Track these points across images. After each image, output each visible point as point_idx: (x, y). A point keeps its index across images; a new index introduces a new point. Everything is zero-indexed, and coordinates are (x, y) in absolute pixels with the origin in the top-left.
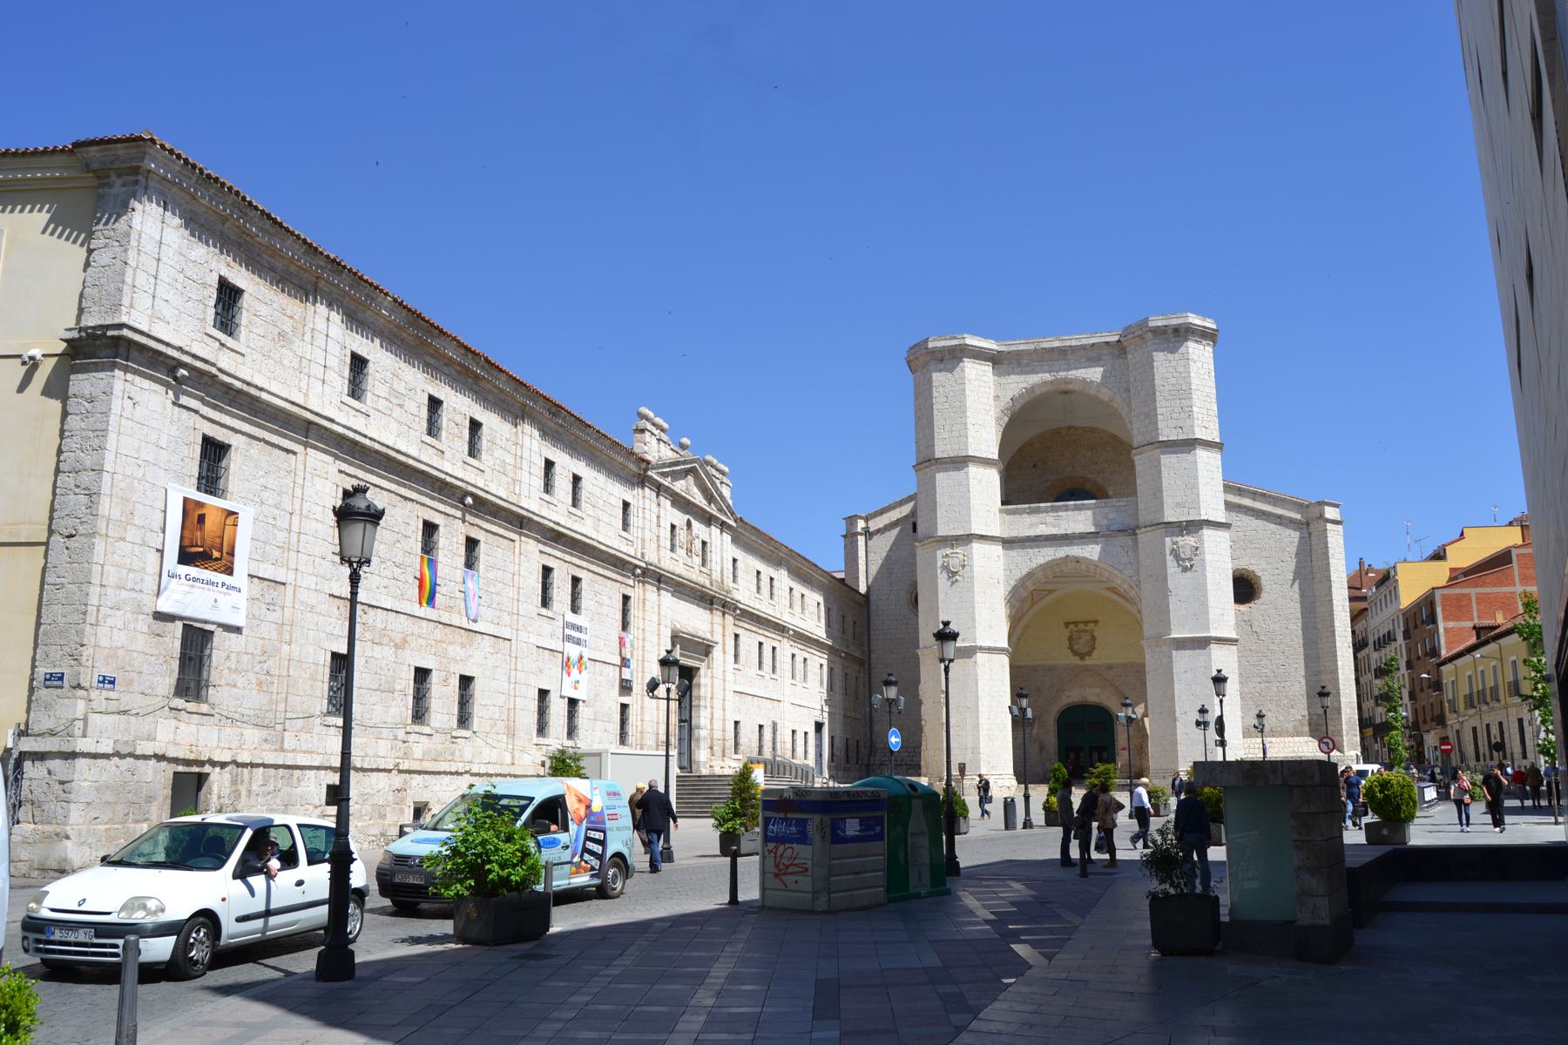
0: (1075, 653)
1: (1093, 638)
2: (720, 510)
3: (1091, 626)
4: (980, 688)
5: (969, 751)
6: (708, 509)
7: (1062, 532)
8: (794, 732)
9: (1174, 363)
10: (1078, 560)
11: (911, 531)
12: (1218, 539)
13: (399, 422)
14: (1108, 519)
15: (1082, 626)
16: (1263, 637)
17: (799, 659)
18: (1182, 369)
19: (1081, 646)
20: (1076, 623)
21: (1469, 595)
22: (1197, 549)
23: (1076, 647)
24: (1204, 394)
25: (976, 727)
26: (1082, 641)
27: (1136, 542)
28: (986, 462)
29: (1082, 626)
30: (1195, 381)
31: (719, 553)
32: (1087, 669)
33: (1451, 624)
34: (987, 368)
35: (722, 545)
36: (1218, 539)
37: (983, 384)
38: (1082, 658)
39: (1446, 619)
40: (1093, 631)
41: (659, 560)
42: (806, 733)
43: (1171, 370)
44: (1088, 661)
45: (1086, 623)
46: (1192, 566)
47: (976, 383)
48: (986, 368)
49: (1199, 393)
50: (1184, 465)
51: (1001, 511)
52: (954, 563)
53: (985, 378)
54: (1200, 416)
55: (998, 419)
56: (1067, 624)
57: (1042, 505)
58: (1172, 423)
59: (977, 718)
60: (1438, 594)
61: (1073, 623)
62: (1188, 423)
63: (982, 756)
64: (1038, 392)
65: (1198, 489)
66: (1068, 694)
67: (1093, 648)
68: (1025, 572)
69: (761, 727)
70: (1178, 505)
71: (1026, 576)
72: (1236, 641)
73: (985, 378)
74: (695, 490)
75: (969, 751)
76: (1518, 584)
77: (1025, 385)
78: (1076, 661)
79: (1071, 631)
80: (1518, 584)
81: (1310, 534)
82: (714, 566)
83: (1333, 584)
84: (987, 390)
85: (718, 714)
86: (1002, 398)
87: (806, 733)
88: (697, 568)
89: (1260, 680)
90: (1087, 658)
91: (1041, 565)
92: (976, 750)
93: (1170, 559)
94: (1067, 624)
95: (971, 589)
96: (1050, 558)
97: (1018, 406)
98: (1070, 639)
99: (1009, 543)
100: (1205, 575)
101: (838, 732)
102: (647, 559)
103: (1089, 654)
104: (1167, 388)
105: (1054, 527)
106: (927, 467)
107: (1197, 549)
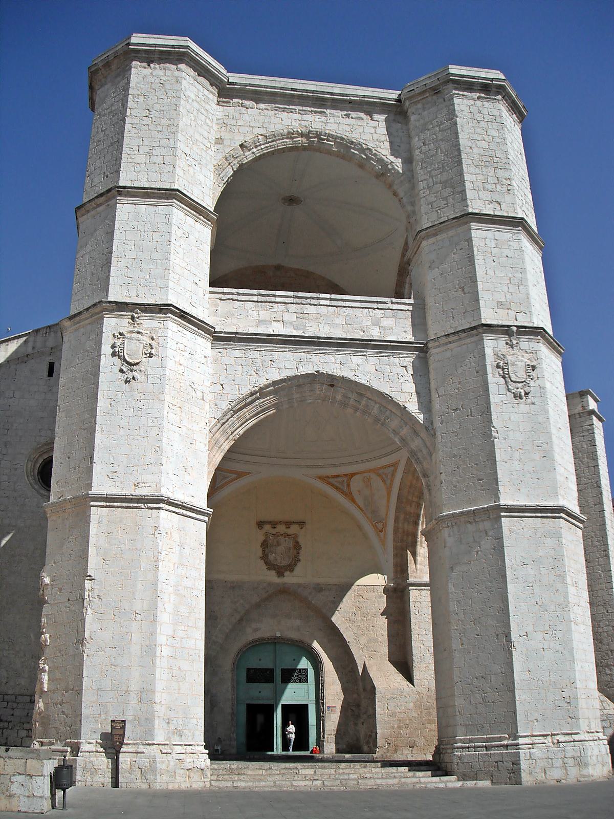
0: (270, 566)
1: (297, 546)
3: (294, 529)
4: (162, 575)
5: (133, 699)
9: (483, 124)
11: (46, 373)
15: (281, 529)
18: (495, 134)
19: (279, 556)
20: (274, 524)
22: (534, 368)
23: (271, 557)
25: (150, 650)
26: (280, 549)
29: (281, 529)
30: (512, 155)
32: (284, 591)
34: (211, 95)
37: (204, 112)
38: (280, 574)
40: (296, 536)
44: (289, 579)
45: (288, 524)
46: (527, 394)
47: (195, 104)
48: (211, 96)
50: (506, 252)
52: (133, 349)
55: (219, 168)
56: (260, 524)
58: (486, 196)
59: (153, 634)
61: (269, 523)
62: (508, 198)
63: (157, 707)
64: (280, 144)
65: (526, 286)
66: (254, 625)
67: (296, 560)
70: (500, 304)
73: (208, 107)
75: (133, 699)
78: (272, 577)
79: (266, 534)
86: (226, 143)
90: (287, 573)
92: (146, 695)
93: (494, 380)
94: (260, 524)
95: (157, 397)
97: (249, 156)
98: (265, 545)
99: (220, 339)
100: (547, 412)
103: (291, 568)
104: (475, 150)
106: (101, 204)
107: (534, 368)
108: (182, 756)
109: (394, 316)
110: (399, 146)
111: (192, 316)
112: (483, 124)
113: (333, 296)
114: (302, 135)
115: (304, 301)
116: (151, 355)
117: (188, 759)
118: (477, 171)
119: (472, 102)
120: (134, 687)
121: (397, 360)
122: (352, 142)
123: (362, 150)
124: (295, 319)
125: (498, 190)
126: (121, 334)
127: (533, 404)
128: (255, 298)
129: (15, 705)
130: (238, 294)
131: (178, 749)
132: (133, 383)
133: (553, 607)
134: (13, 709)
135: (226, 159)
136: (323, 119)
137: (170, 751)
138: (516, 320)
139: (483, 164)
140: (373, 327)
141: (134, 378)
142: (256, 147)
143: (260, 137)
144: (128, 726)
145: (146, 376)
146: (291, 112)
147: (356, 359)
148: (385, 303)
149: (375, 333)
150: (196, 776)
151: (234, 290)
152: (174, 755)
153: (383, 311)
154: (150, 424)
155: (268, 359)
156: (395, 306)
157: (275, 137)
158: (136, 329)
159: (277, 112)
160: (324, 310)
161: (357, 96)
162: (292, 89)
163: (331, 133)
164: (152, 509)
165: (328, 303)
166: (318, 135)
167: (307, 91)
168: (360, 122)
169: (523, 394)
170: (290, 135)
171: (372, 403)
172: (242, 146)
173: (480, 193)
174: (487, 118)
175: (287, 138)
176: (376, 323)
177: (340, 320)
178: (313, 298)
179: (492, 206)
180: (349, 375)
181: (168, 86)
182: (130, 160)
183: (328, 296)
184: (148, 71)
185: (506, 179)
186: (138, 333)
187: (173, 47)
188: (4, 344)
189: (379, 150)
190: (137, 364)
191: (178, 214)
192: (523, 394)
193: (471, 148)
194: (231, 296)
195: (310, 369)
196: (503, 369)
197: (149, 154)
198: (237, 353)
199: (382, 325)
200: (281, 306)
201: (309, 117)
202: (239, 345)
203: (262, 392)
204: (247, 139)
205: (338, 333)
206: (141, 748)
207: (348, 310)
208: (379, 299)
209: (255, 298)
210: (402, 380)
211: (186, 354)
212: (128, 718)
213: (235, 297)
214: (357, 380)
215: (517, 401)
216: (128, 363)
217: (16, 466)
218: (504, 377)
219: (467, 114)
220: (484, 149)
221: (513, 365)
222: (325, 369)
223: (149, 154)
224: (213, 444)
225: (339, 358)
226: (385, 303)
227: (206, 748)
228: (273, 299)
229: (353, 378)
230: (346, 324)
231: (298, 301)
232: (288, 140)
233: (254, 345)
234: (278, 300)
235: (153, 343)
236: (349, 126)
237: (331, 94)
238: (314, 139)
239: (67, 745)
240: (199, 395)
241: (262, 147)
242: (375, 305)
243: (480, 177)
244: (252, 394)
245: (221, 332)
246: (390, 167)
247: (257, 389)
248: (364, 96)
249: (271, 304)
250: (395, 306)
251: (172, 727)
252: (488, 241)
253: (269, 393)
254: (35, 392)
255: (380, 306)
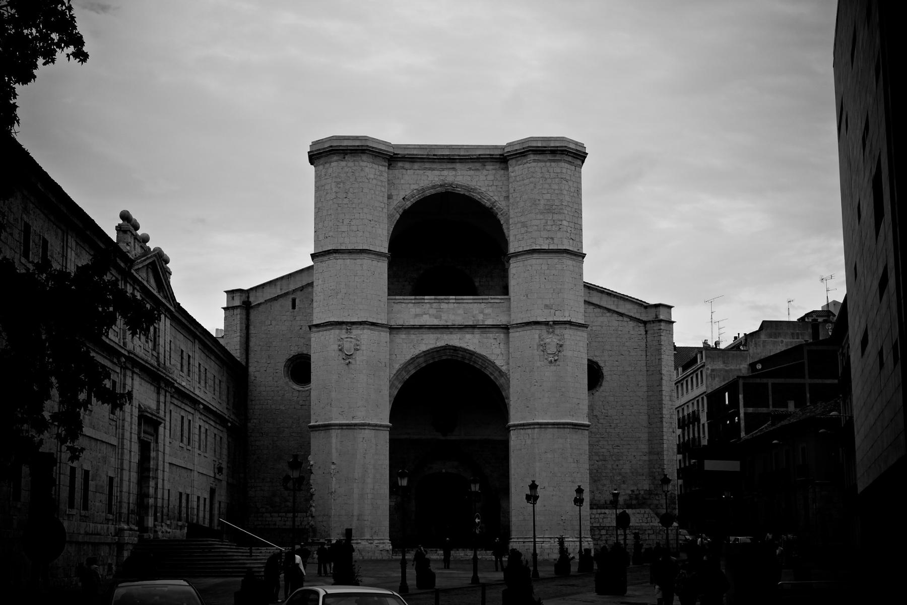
2: (166, 297)
5: (355, 518)
6: (159, 296)
7: (442, 323)
8: (198, 498)
10: (455, 349)
11: (290, 307)
12: (578, 338)
13: (11, 248)
14: (484, 314)
16: (601, 421)
17: (203, 430)
18: (556, 187)
21: (767, 384)
22: (561, 346)
24: (573, 210)
27: (508, 333)
28: (379, 254)
31: (163, 338)
33: (750, 410)
35: (165, 330)
36: (578, 338)
37: (379, 183)
39: (745, 406)
41: (134, 349)
42: (205, 499)
43: (546, 186)
47: (374, 182)
49: (569, 209)
50: (553, 272)
51: (388, 299)
53: (382, 178)
54: (569, 229)
55: (390, 216)
57: (426, 297)
58: (545, 234)
60: (741, 382)
62: (559, 235)
64: (428, 193)
68: (408, 357)
69: (181, 494)
71: (409, 361)
72: (588, 426)
73: (382, 178)
74: (152, 281)
75: (355, 518)
76: (807, 376)
77: (416, 187)
80: (807, 376)
81: (646, 332)
82: (162, 350)
83: (664, 378)
84: (383, 189)
85: (160, 486)
87: (205, 499)
88: (150, 351)
89: (598, 459)
91: (424, 352)
96: (432, 346)
97: (408, 204)
101: (223, 497)
102: (128, 348)
104: (542, 202)
105: (436, 318)
108: (378, 544)
109: (491, 307)
110: (501, 188)
111: (378, 323)
112: (549, 181)
113: (457, 297)
114: (441, 186)
115: (441, 301)
116: (358, 350)
117: (381, 546)
118: (541, 217)
119: (543, 164)
120: (355, 513)
121: (491, 335)
122: (472, 188)
123: (479, 193)
124: (435, 312)
125: (553, 229)
126: (342, 339)
127: (559, 365)
128: (413, 301)
129: (286, 519)
130: (404, 299)
131: (376, 542)
132: (350, 365)
133: (559, 475)
134: (285, 521)
135: (395, 209)
136: (454, 173)
137: (372, 542)
138: (555, 315)
139: (546, 211)
140: (480, 315)
141: (349, 362)
142: (413, 197)
143: (415, 191)
144: (353, 532)
145: (356, 361)
146: (434, 170)
147: (468, 336)
148: (488, 299)
149: (480, 319)
150: (384, 553)
151: (401, 297)
152: (374, 544)
153: (485, 304)
154: (359, 386)
155: (420, 339)
156: (492, 301)
157: (423, 190)
158: (349, 336)
159: (425, 171)
160: (451, 306)
161: (475, 155)
162: (434, 155)
163: (459, 183)
164: (361, 429)
165: (454, 301)
166: (451, 185)
167: (443, 155)
168: (477, 173)
169: (553, 361)
170: (434, 187)
171: (478, 359)
172: (403, 199)
173: (542, 233)
174: (552, 175)
175: (432, 189)
176: (482, 312)
177: (461, 311)
178: (446, 299)
179: (548, 241)
180: (464, 345)
181: (357, 174)
182: (339, 230)
183: (454, 297)
184: (343, 164)
185: (559, 221)
186: (351, 338)
187: (358, 146)
188: (261, 287)
189: (488, 193)
190: (351, 355)
191: (366, 262)
192: (553, 361)
193: (539, 200)
194: (400, 301)
195: (441, 343)
196: (543, 347)
197: (349, 225)
198: (403, 336)
199: (485, 313)
200: (428, 305)
201: (445, 173)
202: (404, 332)
203: (417, 357)
204: (407, 193)
205: (459, 320)
206: (359, 541)
207: (464, 305)
208: (483, 297)
209: (413, 301)
210: (493, 347)
211: (376, 345)
212: (353, 527)
213: (402, 301)
214: (468, 348)
215: (550, 365)
216: (348, 355)
217: (276, 371)
218: (543, 351)
219: (539, 174)
220: (548, 200)
221: (549, 344)
222: (451, 343)
223: (349, 225)
224: (392, 386)
225: (459, 336)
226: (488, 299)
227: (390, 541)
228: (423, 301)
229: (466, 348)
230: (464, 313)
231: (437, 301)
232: (432, 190)
233: (412, 331)
234: (426, 301)
235: (358, 343)
236: (469, 177)
237: (459, 155)
238: (448, 188)
239: (326, 540)
240: (384, 364)
241: (417, 197)
242: (481, 301)
243: (543, 221)
244: (412, 359)
245: (394, 325)
246: (495, 204)
247: (414, 356)
248: (480, 155)
249: (422, 304)
250: (492, 301)
251: (374, 531)
252: (543, 266)
253: (421, 357)
254: (285, 321)
255: (484, 301)
